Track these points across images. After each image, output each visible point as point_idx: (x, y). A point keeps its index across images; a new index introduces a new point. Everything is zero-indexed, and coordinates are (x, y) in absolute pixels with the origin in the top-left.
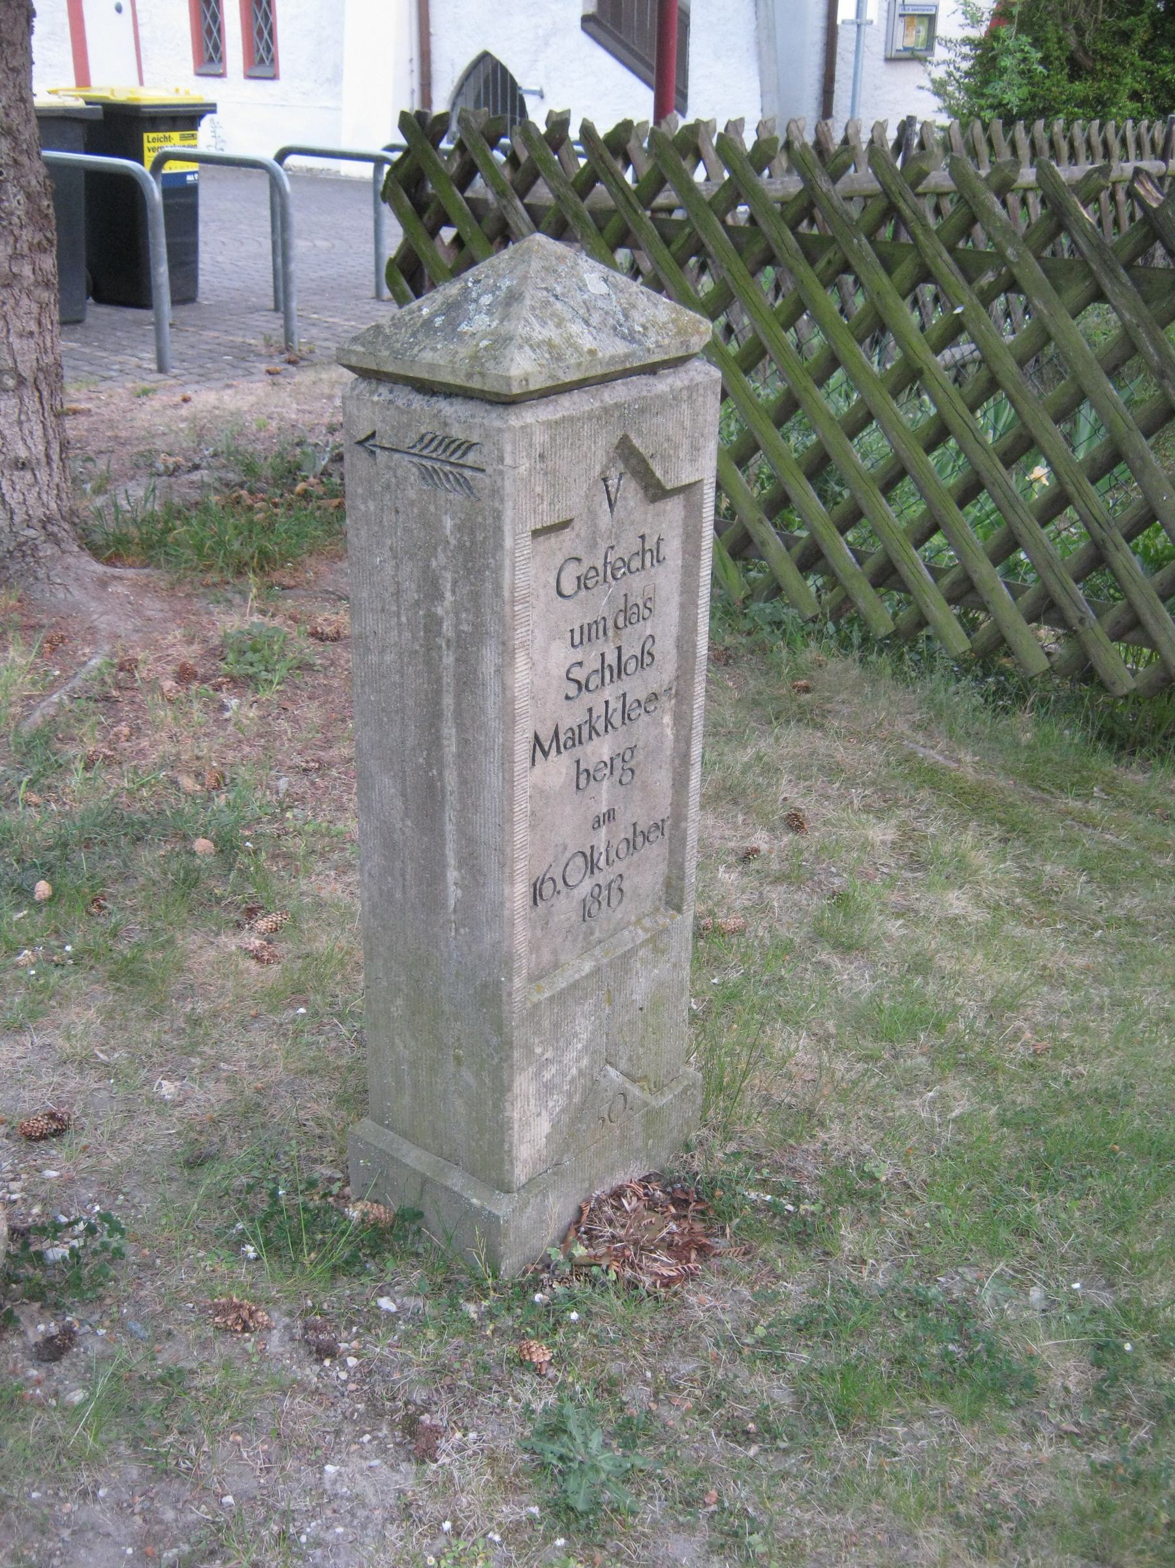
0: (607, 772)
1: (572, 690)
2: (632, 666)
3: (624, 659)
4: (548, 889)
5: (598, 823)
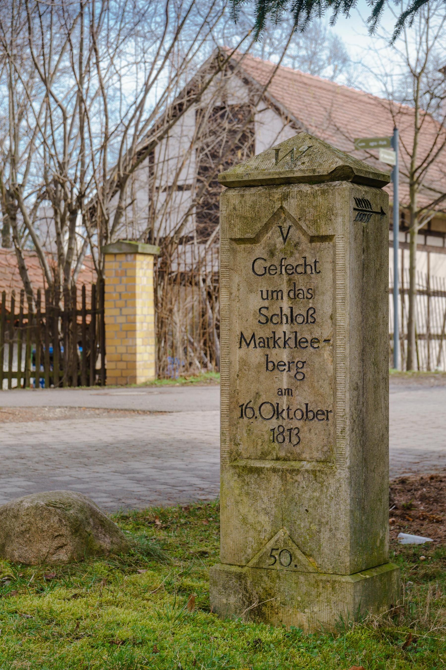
0: (286, 368)
1: (263, 320)
2: (300, 320)
3: (295, 315)
4: (249, 413)
5: (280, 392)
